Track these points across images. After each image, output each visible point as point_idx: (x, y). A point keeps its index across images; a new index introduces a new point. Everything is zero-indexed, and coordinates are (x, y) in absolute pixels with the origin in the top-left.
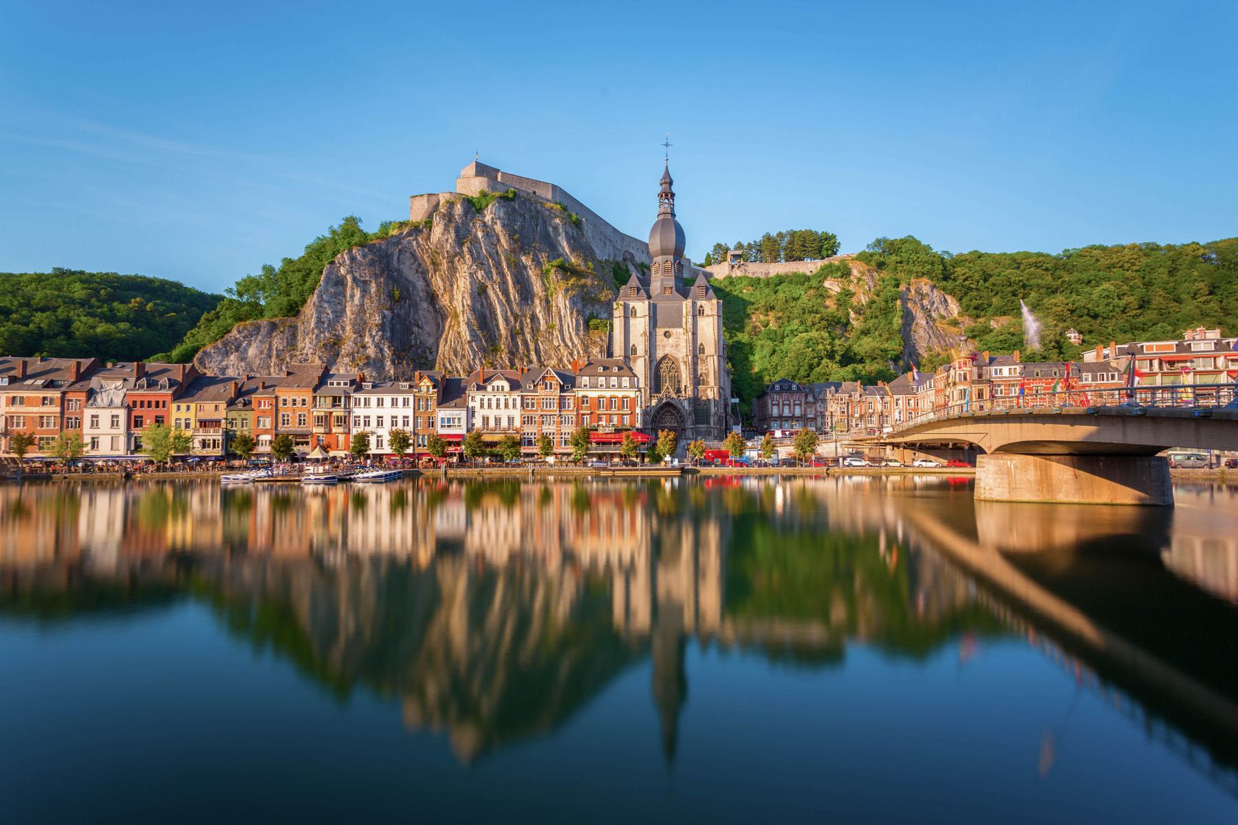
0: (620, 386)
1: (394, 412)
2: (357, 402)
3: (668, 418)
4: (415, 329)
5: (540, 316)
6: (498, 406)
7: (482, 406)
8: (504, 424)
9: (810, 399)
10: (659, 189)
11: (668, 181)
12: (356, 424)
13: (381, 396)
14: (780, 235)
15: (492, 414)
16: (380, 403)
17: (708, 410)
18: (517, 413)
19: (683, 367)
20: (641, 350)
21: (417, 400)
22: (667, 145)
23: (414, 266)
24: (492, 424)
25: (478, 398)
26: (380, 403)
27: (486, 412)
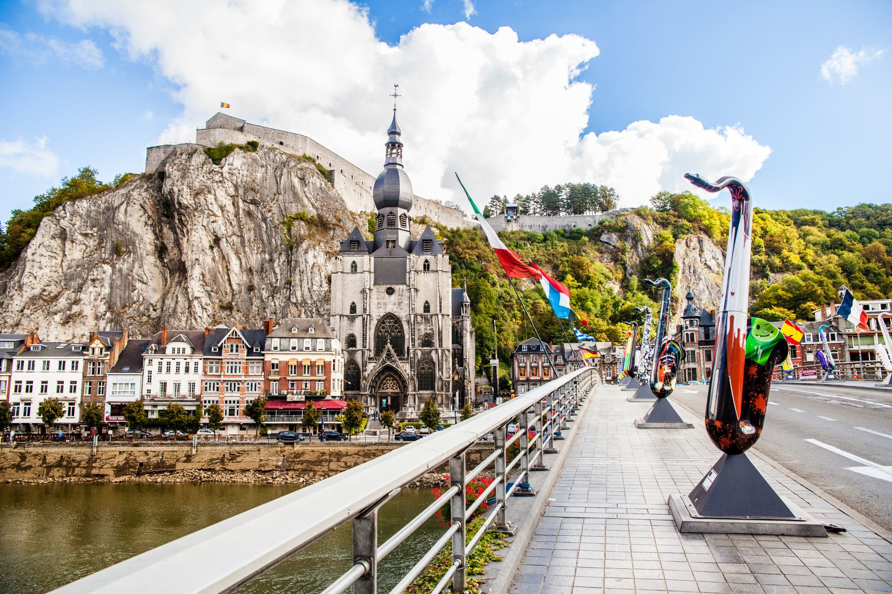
0: (314, 350)
1: (61, 376)
2: (21, 365)
3: (390, 383)
4: (138, 285)
5: (278, 270)
6: (178, 370)
7: (160, 370)
8: (184, 390)
9: (560, 360)
10: (387, 139)
11: (393, 131)
12: (18, 389)
13: (47, 358)
14: (559, 188)
15: (171, 379)
16: (47, 365)
17: (433, 375)
18: (196, 378)
19: (406, 327)
20: (359, 311)
21: (87, 361)
22: (395, 96)
23: (144, 219)
24: (170, 391)
25: (156, 362)
26: (47, 365)
27: (164, 377)
